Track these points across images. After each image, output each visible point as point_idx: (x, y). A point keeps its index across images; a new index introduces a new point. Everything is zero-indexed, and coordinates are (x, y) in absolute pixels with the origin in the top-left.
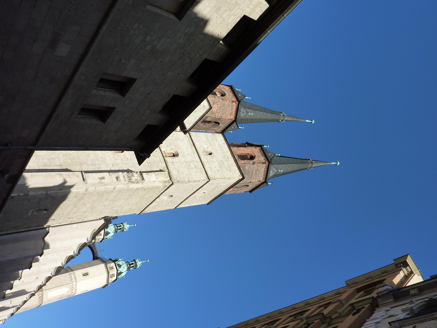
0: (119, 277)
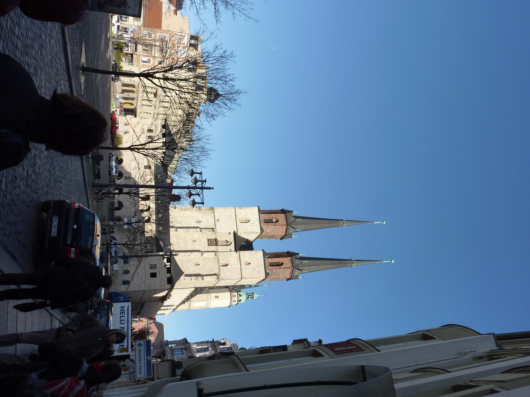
0: (239, 302)
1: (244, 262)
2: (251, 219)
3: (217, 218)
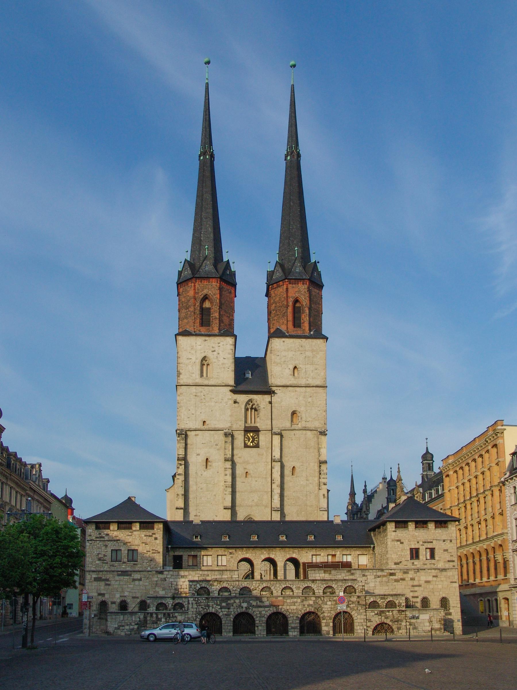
1: (293, 379)
2: (203, 355)
3: (199, 425)
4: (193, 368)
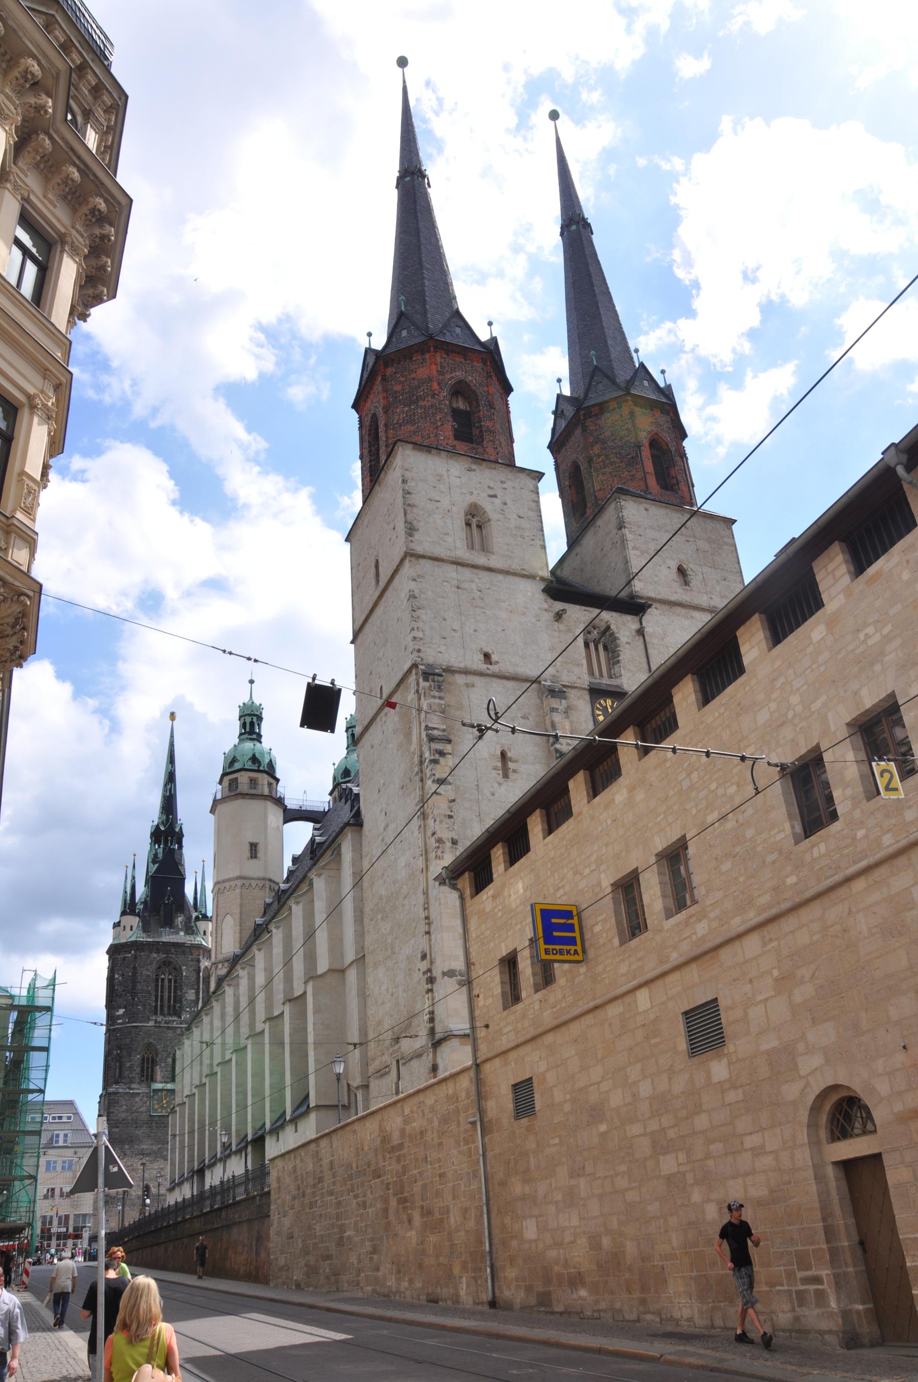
2: (469, 499)
3: (477, 662)
4: (445, 522)
